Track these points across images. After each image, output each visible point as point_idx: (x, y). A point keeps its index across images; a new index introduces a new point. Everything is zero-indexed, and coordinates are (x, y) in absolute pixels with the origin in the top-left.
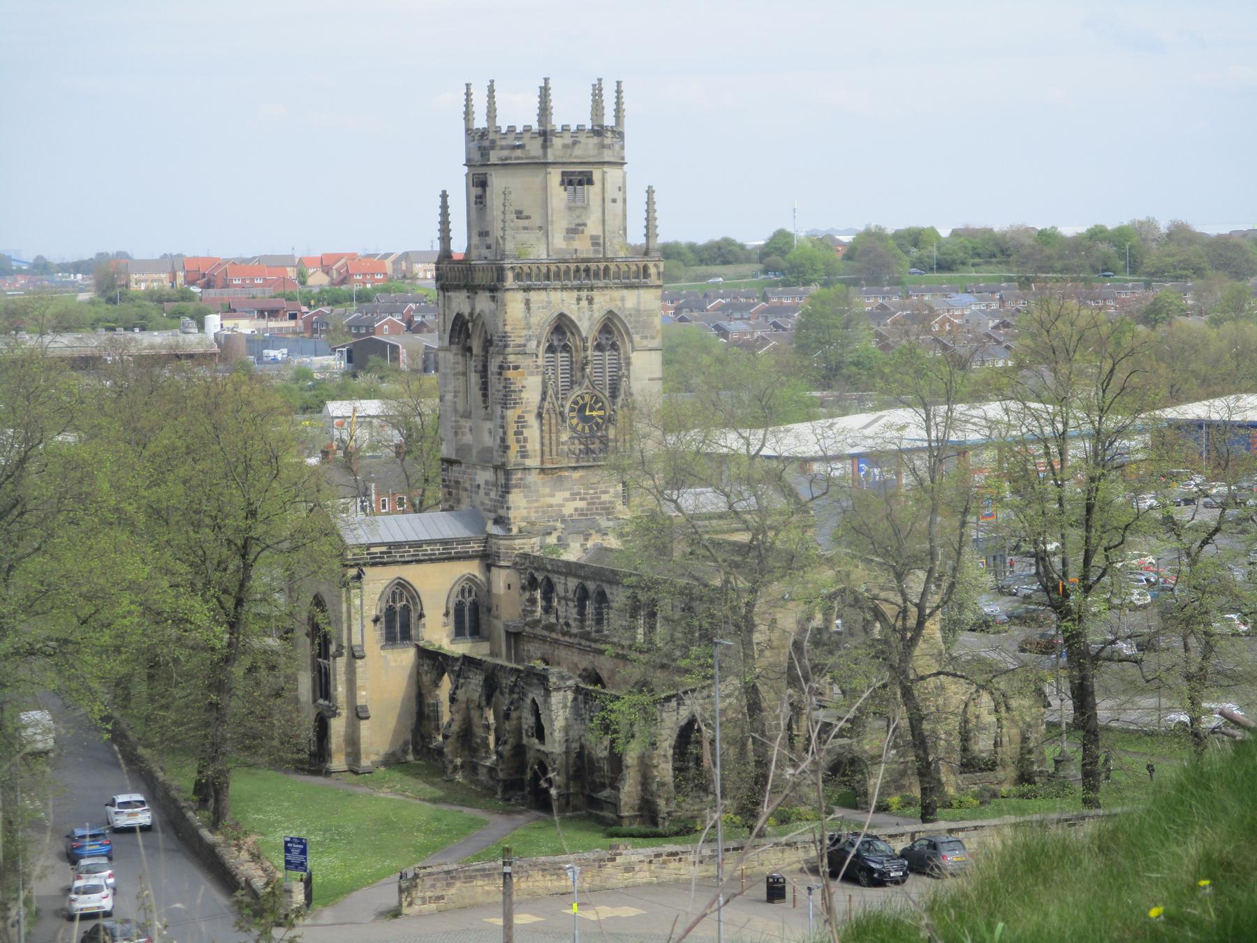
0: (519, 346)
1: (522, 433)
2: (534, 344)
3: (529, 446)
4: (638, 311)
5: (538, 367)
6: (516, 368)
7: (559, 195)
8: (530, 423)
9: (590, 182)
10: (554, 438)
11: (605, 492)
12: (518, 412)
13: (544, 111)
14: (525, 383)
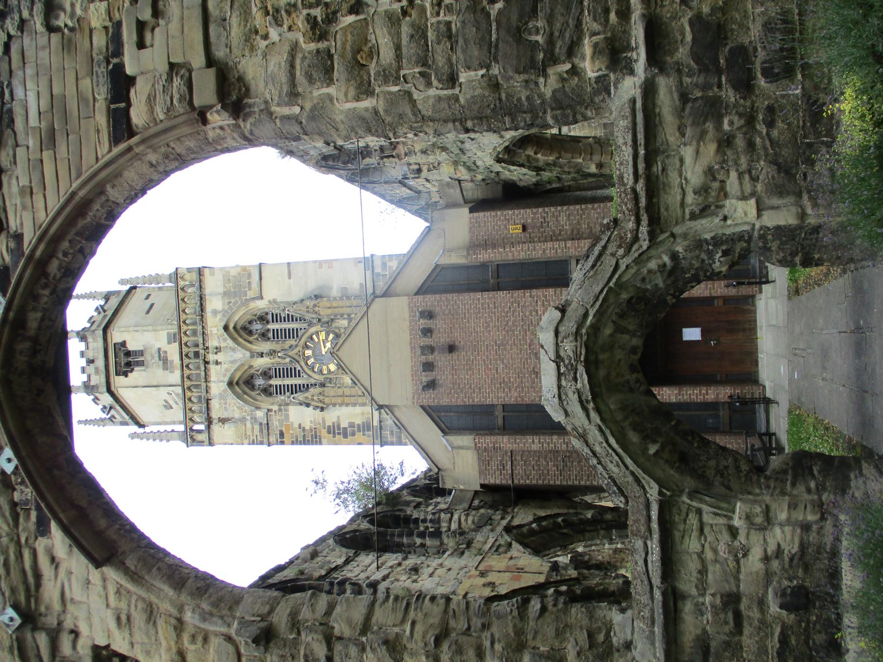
0: (261, 430)
1: (345, 429)
2: (260, 414)
3: (358, 421)
4: (226, 294)
5: (280, 410)
6: (282, 434)
7: (137, 375)
8: (335, 420)
9: (124, 344)
12: (324, 432)
14: (296, 425)
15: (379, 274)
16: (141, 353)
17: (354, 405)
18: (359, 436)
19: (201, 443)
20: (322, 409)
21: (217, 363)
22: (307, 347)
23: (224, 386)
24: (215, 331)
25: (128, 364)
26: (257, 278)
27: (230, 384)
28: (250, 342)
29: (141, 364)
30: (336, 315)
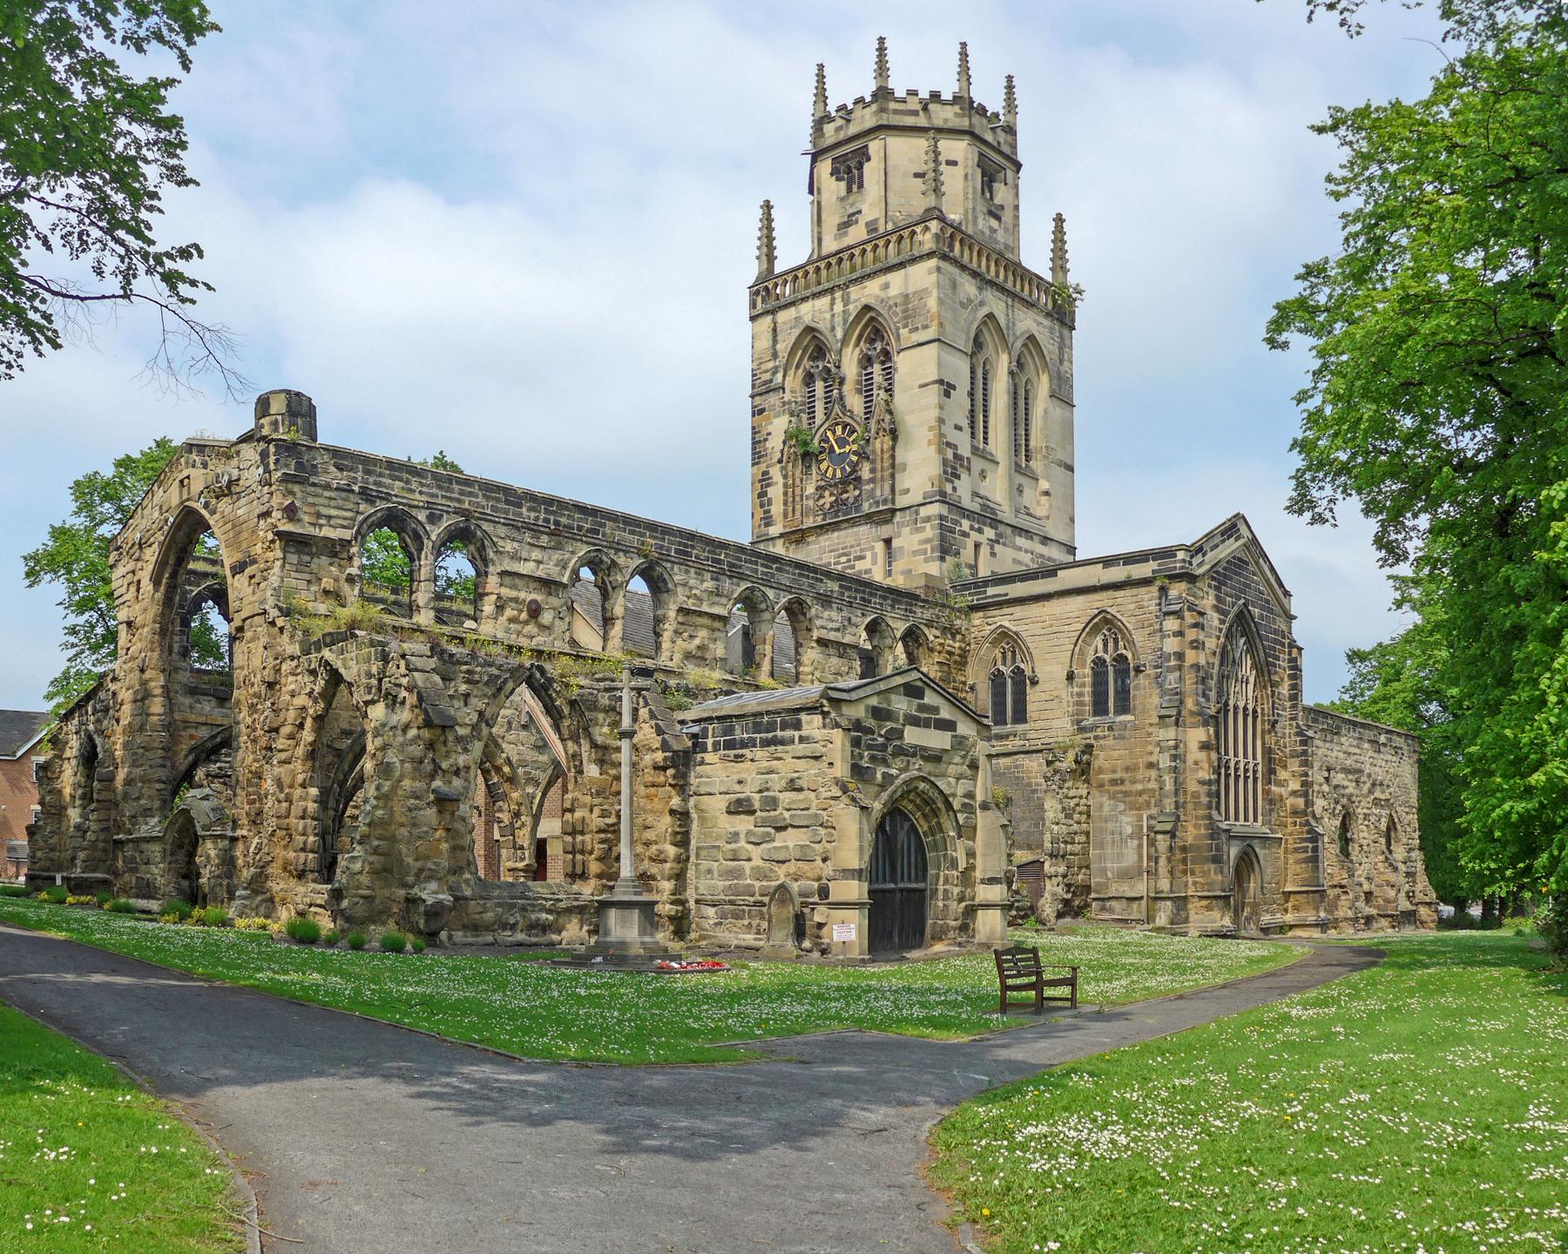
0: (765, 383)
10: (798, 491)
11: (861, 558)
12: (763, 467)
13: (821, 95)
14: (770, 428)
15: (917, 513)
16: (861, 186)
17: (785, 504)
18: (760, 513)
19: (753, 305)
20: (780, 461)
21: (833, 303)
22: (844, 429)
23: (807, 320)
24: (867, 292)
25: (849, 170)
26: (922, 340)
27: (809, 330)
28: (857, 344)
29: (849, 190)
30: (873, 462)
